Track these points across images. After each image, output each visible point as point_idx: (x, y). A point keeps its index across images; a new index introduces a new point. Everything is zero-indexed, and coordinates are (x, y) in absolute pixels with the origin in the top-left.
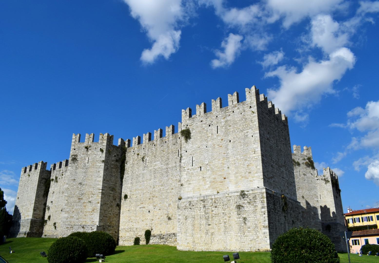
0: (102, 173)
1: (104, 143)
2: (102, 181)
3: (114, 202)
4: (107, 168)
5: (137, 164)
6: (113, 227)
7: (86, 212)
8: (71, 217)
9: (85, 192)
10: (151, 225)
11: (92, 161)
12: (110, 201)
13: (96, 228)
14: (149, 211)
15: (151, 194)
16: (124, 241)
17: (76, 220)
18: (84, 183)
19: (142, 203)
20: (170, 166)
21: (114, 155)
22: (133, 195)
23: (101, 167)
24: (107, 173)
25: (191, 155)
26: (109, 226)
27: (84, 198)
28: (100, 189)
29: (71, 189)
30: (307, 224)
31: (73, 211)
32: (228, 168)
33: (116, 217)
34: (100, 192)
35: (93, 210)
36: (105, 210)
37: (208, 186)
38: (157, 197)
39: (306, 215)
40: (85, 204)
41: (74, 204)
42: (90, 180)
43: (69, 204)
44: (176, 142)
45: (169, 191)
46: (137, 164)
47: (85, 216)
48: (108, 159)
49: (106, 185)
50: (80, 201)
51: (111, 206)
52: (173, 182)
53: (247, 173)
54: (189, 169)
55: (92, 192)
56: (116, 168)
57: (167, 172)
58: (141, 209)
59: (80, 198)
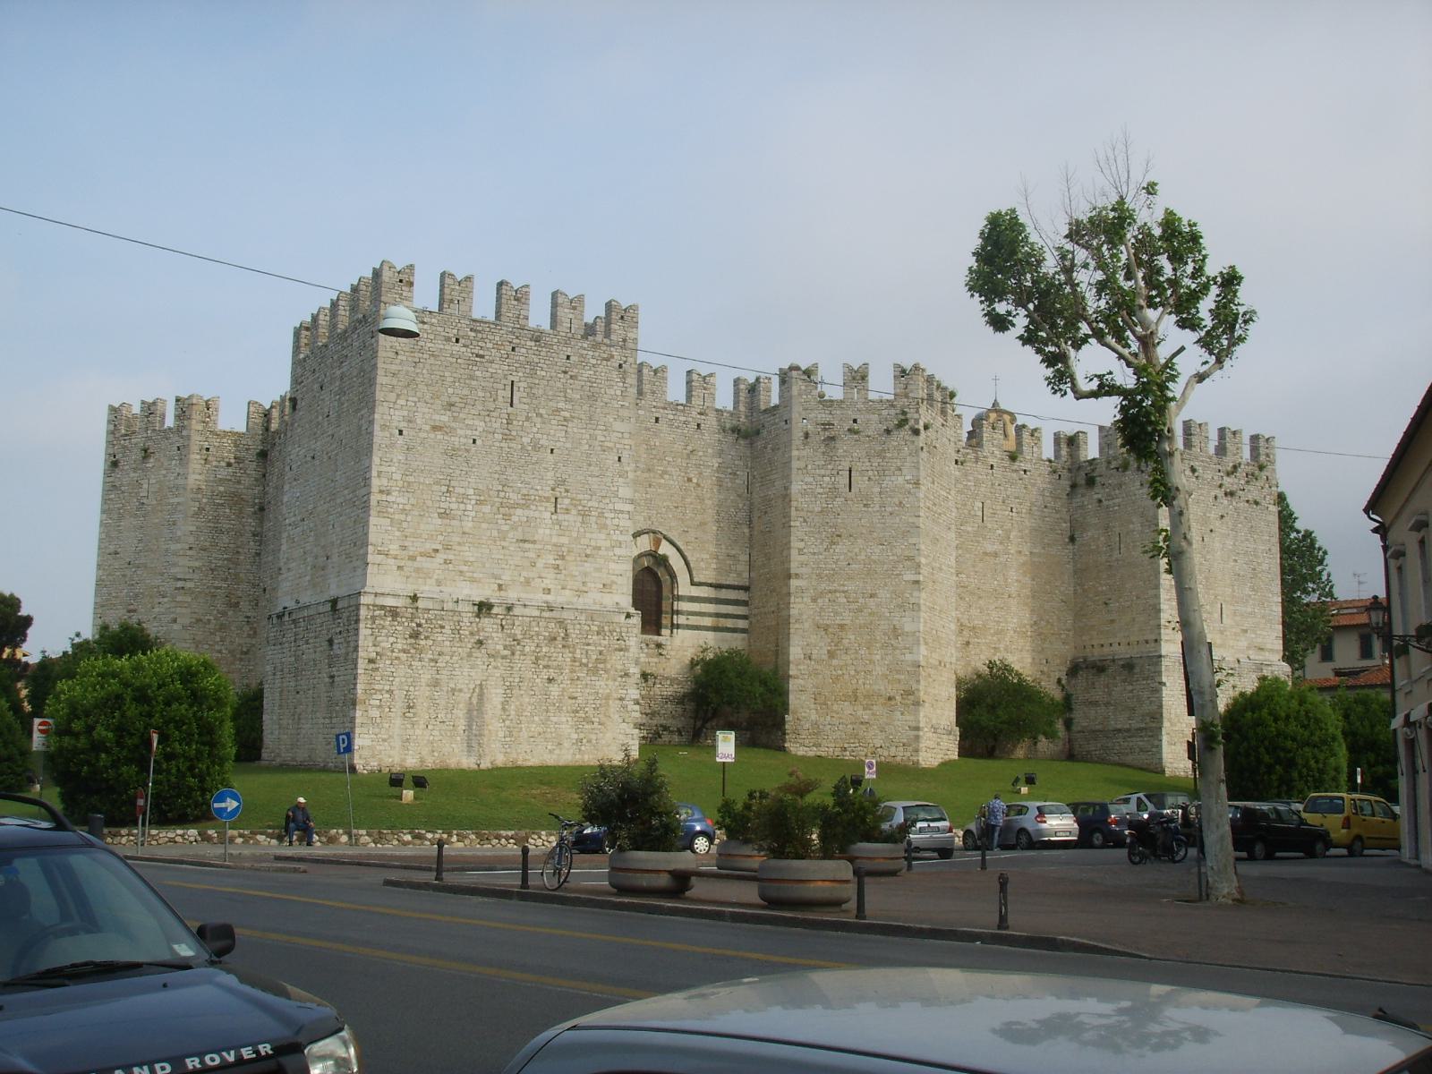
3: (230, 613)
4: (201, 509)
12: (215, 612)
21: (223, 464)
24: (197, 524)
25: (295, 480)
28: (180, 579)
30: (852, 673)
32: (333, 526)
33: (241, 660)
34: (176, 589)
36: (200, 642)
37: (308, 578)
39: (852, 637)
49: (197, 564)
51: (222, 627)
53: (352, 545)
54: (290, 525)
59: (132, 607)
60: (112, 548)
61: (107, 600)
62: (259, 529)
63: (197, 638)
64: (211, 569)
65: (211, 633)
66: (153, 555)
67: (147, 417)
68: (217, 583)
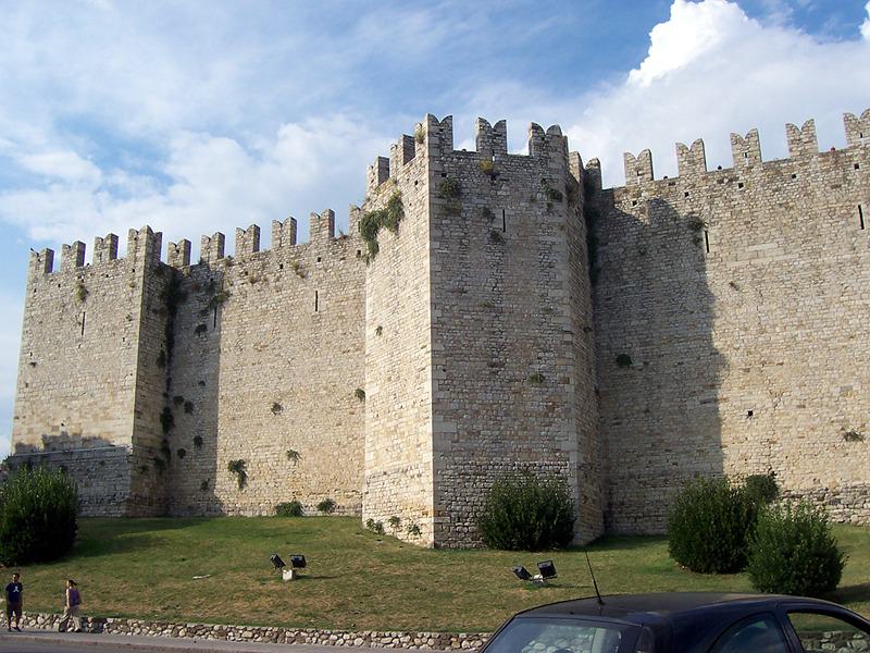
0: (563, 272)
5: (664, 246)
8: (470, 433)
10: (766, 460)
11: (517, 223)
14: (750, 413)
15: (749, 353)
20: (829, 259)
31: (477, 412)
34: (567, 343)
35: (552, 409)
38: (782, 364)
41: (475, 383)
44: (845, 179)
45: (833, 344)
46: (664, 246)
47: (526, 429)
50: (496, 373)
52: (850, 313)
55: (536, 338)
57: (818, 278)
61: (454, 348)
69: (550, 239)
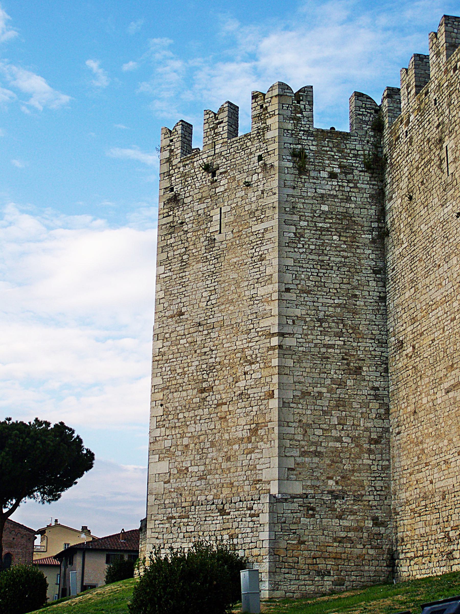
1: (268, 128)
2: (275, 296)
3: (349, 383)
4: (299, 236)
6: (358, 499)
7: (229, 442)
9: (218, 360)
12: (328, 381)
13: (266, 508)
16: (411, 559)
17: (198, 483)
18: (213, 320)
19: (452, 366)
21: (324, 174)
22: (422, 334)
23: (267, 236)
26: (336, 497)
27: (217, 382)
28: (273, 335)
29: (173, 354)
33: (370, 451)
34: (272, 348)
36: (309, 425)
40: (225, 408)
41: (186, 414)
42: (231, 302)
43: (171, 417)
47: (228, 459)
48: (296, 192)
49: (298, 312)
50: (204, 399)
56: (346, 229)
58: (451, 394)
59: (204, 385)
60: (174, 308)
62: (380, 264)
63: (304, 421)
64: (319, 320)
65: (325, 413)
66: (231, 308)
67: (214, 128)
68: (327, 340)
69: (261, 227)
